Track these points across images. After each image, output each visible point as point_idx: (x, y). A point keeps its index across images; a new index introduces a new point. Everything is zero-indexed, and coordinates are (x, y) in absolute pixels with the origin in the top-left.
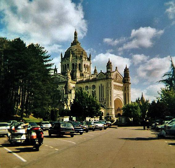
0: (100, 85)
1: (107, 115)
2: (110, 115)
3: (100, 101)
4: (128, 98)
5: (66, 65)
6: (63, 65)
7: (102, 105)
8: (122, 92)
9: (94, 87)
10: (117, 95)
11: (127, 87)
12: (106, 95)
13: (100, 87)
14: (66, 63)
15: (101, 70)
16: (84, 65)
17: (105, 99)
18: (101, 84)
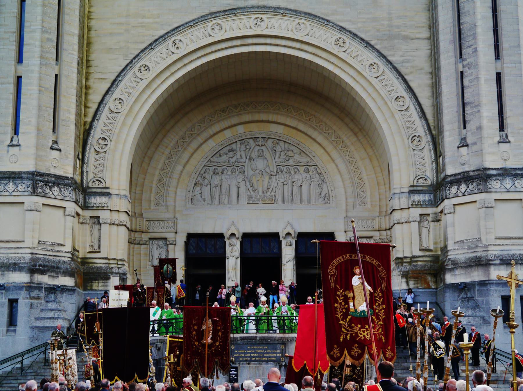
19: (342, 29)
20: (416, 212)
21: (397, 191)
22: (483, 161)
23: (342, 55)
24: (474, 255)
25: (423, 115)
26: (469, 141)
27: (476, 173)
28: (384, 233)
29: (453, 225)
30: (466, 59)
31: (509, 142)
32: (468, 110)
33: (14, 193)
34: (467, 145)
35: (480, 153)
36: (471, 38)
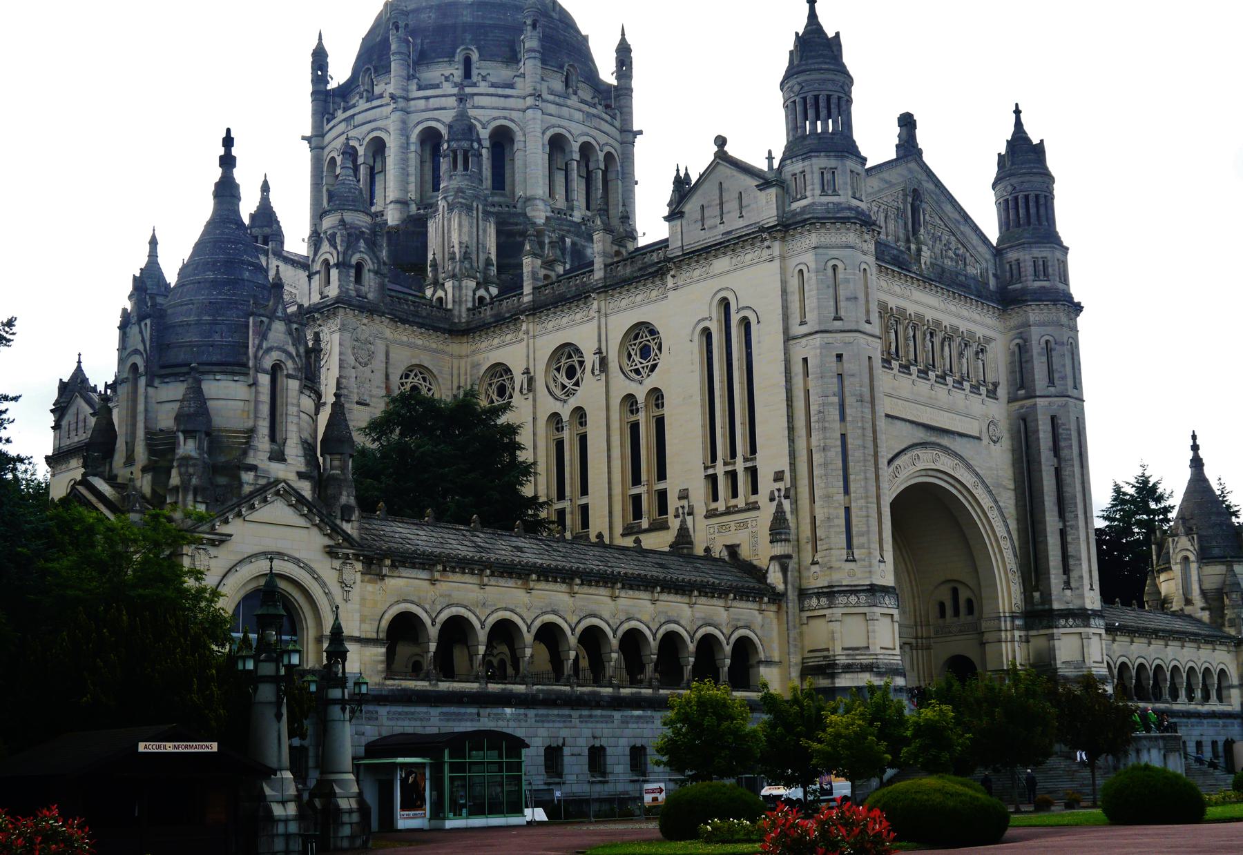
0: (716, 313)
1: (807, 671)
2: (848, 668)
3: (711, 514)
4: (1058, 472)
5: (361, 151)
6: (333, 160)
7: (745, 553)
8: (998, 410)
9: (645, 352)
10: (921, 435)
11: (1036, 349)
12: (791, 429)
13: (707, 333)
14: (360, 138)
15: (721, 141)
16: (557, 144)
17: (779, 477)
18: (726, 304)
19: (977, 474)
20: (1017, 633)
21: (1002, 615)
22: (1084, 603)
23: (977, 496)
24: (1081, 673)
25: (1015, 556)
26: (1073, 585)
27: (1080, 611)
28: (920, 641)
29: (1059, 649)
30: (1068, 521)
31: (1093, 590)
32: (1071, 562)
33: (890, 606)
34: (1071, 589)
35: (1082, 597)
36: (1073, 506)
